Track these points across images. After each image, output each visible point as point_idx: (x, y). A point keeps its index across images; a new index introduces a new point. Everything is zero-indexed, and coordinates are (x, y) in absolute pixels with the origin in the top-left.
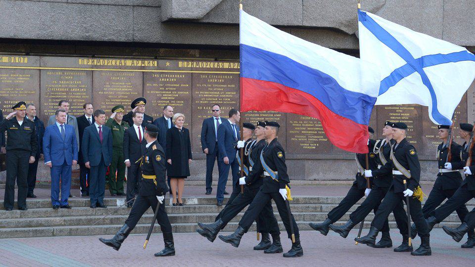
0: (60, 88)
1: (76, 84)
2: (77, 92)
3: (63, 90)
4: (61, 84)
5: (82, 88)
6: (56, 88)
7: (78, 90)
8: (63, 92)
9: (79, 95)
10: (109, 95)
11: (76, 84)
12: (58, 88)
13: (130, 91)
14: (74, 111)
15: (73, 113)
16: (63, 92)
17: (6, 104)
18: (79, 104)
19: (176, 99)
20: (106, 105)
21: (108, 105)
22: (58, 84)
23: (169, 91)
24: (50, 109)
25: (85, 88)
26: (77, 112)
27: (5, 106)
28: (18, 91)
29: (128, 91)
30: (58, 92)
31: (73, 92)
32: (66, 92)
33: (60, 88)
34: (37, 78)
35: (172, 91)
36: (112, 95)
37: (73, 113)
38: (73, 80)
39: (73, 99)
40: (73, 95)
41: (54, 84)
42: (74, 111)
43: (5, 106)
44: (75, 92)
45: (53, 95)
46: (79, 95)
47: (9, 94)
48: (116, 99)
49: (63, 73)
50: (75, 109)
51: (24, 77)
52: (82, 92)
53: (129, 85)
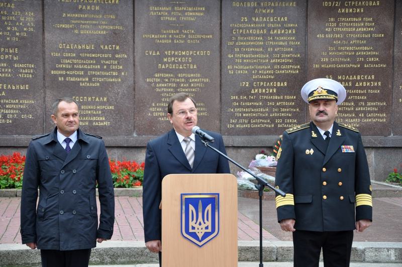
0: (253, 28)
1: (279, 23)
2: (281, 35)
3: (258, 32)
4: (255, 23)
5: (289, 28)
6: (246, 28)
7: (283, 31)
8: (258, 36)
9: (284, 41)
10: (335, 39)
11: (279, 23)
12: (249, 29)
13: (370, 32)
14: (275, 67)
15: (275, 73)
16: (258, 36)
17: (167, 56)
18: (283, 56)
20: (329, 57)
21: (333, 56)
22: (250, 22)
24: (237, 64)
25: (293, 28)
26: (280, 69)
27: (165, 60)
28: (187, 35)
30: (250, 35)
31: (273, 36)
32: (263, 35)
33: (253, 28)
34: (216, 12)
36: (339, 39)
38: (273, 15)
39: (274, 47)
40: (274, 40)
41: (244, 22)
42: (275, 67)
43: (165, 60)
44: (277, 35)
45: (241, 41)
46: (284, 41)
47: (173, 39)
48: (346, 45)
50: (279, 64)
51: (195, 11)
52: (289, 35)
53: (369, 22)
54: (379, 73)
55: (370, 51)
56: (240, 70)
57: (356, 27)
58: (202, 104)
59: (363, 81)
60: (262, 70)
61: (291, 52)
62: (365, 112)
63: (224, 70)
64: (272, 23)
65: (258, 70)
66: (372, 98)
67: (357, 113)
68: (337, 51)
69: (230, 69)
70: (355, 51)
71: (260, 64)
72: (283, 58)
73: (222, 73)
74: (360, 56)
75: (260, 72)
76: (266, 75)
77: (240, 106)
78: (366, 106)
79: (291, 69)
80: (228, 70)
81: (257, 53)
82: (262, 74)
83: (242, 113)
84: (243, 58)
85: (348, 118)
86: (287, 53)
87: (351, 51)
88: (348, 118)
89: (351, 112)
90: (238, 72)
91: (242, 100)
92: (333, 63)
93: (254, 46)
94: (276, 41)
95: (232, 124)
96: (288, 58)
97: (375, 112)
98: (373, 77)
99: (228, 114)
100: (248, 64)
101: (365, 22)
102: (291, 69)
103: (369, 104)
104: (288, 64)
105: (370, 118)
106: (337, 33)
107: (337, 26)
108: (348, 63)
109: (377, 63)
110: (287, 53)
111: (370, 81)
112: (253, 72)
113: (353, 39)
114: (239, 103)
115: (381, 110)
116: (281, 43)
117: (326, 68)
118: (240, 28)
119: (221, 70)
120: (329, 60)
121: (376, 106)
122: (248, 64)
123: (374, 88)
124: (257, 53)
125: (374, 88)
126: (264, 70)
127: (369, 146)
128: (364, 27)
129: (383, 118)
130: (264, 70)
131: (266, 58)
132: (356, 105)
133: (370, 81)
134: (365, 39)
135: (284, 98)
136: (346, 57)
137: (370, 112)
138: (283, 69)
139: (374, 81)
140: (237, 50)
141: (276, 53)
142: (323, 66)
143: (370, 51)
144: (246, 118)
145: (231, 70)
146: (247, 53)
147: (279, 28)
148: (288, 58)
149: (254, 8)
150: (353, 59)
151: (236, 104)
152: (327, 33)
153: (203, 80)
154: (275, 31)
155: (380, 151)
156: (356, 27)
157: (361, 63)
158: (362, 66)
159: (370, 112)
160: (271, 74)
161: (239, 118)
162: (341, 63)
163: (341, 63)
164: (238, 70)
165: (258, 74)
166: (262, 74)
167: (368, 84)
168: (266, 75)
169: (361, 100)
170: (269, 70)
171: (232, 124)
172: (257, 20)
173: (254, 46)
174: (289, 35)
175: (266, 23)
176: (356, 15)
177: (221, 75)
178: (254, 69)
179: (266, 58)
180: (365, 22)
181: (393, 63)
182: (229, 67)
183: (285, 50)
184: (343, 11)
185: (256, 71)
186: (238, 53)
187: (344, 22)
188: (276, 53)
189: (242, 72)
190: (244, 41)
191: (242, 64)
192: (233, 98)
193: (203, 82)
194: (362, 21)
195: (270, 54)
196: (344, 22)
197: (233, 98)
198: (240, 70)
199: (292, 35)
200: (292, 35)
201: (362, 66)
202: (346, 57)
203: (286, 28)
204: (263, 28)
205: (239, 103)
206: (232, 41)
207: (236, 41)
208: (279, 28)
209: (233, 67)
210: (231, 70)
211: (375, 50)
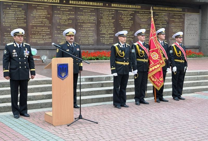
0: (11, 11)
1: (19, 10)
5: (22, 12)
9: (21, 16)
10: (36, 16)
11: (19, 10)
13: (46, 15)
14: (18, 24)
16: (13, 14)
18: (21, 21)
19: (69, 19)
21: (36, 21)
23: (65, 15)
24: (6, 23)
29: (45, 15)
30: (10, 13)
31: (17, 14)
32: (14, 14)
33: (11, 11)
35: (66, 15)
36: (37, 16)
39: (18, 18)
40: (18, 16)
41: (8, 9)
42: (18, 24)
45: (7, 15)
46: (21, 16)
49: (12, 4)
52: (22, 14)
54: (49, 27)
55: (46, 20)
57: (42, 13)
59: (44, 29)
61: (23, 20)
62: (45, 39)
64: (17, 10)
65: (13, 25)
66: (47, 34)
67: (43, 39)
68: (37, 20)
70: (42, 20)
71: (13, 23)
72: (21, 21)
74: (44, 22)
75: (14, 25)
76: (15, 26)
77: (7, 36)
78: (46, 37)
79: (23, 25)
80: (3, 25)
81: (12, 19)
82: (14, 26)
83: (8, 38)
84: (8, 21)
85: (41, 40)
86: (22, 20)
87: (41, 20)
88: (41, 40)
89: (41, 39)
91: (8, 34)
92: (36, 23)
93: (11, 17)
94: (18, 16)
95: (5, 42)
96: (22, 21)
97: (48, 39)
98: (47, 28)
100: (10, 23)
101: (44, 12)
102: (23, 25)
103: (46, 36)
104: (23, 23)
105: (47, 40)
106: (37, 14)
107: (37, 12)
108: (40, 24)
109: (48, 24)
110: (22, 20)
111: (46, 29)
113: (41, 16)
114: (7, 35)
115: (50, 38)
116: (20, 17)
117: (34, 25)
118: (6, 11)
120: (35, 23)
121: (48, 37)
122: (10, 23)
123: (48, 32)
124: (12, 19)
125: (48, 32)
126: (15, 25)
127: (47, 49)
128: (44, 13)
129: (51, 40)
131: (15, 21)
132: (43, 37)
133: (46, 29)
134: (45, 17)
136: (40, 22)
137: (47, 39)
139: (48, 29)
140: (6, 18)
141: (18, 20)
142: (33, 24)
143: (46, 20)
144: (9, 40)
146: (9, 19)
147: (19, 12)
148: (22, 21)
149: (11, 5)
150: (42, 22)
151: (6, 35)
152: (34, 14)
154: (18, 13)
155: (50, 50)
156: (42, 13)
157: (44, 24)
158: (44, 25)
159: (47, 39)
160: (17, 26)
161: (7, 40)
162: (38, 24)
163: (38, 24)
165: (13, 26)
166: (14, 26)
167: (46, 30)
168: (15, 26)
169: (44, 35)
170: (16, 25)
171: (5, 42)
172: (12, 9)
173: (11, 17)
174: (22, 14)
175: (15, 10)
176: (42, 9)
178: (12, 25)
179: (15, 21)
180: (44, 12)
181: (53, 24)
183: (21, 19)
184: (38, 8)
186: (6, 19)
187: (39, 11)
188: (18, 20)
190: (8, 15)
191: (8, 23)
192: (5, 33)
194: (44, 11)
195: (17, 20)
196: (39, 11)
197: (5, 33)
199: (23, 14)
200: (23, 14)
201: (44, 25)
202: (40, 22)
203: (21, 12)
204: (14, 12)
205: (7, 35)
206: (4, 15)
207: (6, 15)
208: (19, 12)
211: (48, 20)
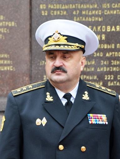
37: (103, 10)
56: (57, 10)
58: (6, 56)
60: (86, 10)
63: (35, 11)
65: (81, 10)
69: (43, 10)
73: (33, 14)
75: (84, 13)
80: (40, 11)
90: (53, 13)
99: (40, 68)
112: (74, 13)
119: (31, 11)
126: (89, 9)
130: (89, 9)
135: (116, 46)
138: (114, 9)
145: (44, 10)
153: (7, 23)
164: (54, 10)
170: (96, 9)
177: (31, 17)
178: (75, 9)
182: (41, 7)
185: (78, 12)
189: (59, 13)
193: (7, 27)
198: (57, 10)
209: (47, 7)
210: (44, 10)
